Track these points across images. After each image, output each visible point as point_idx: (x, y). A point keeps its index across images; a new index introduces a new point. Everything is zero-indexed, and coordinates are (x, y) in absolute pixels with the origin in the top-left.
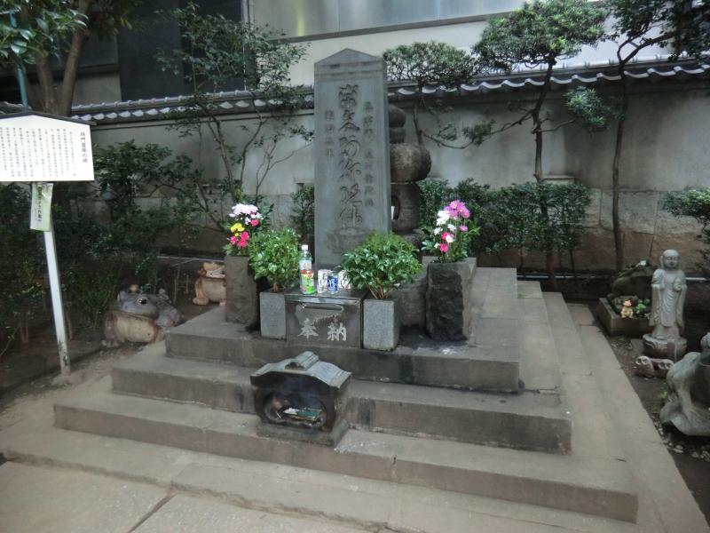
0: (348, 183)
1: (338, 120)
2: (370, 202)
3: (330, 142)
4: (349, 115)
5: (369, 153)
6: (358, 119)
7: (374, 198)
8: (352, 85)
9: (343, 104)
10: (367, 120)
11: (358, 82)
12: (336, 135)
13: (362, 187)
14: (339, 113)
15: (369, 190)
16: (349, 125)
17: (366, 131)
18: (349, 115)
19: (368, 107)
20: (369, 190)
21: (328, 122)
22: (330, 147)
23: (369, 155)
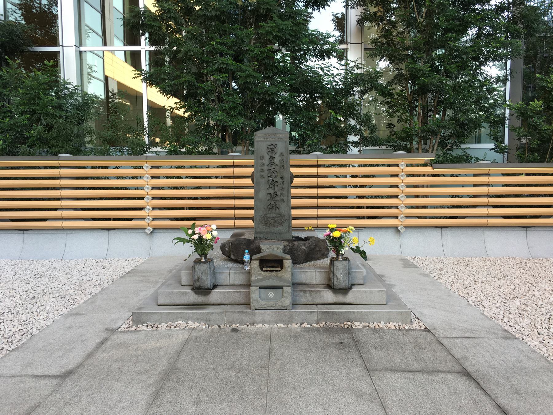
0: (271, 191)
1: (267, 161)
2: (283, 201)
3: (262, 171)
4: (272, 158)
5: (282, 177)
6: (277, 160)
7: (284, 198)
8: (274, 144)
9: (269, 153)
10: (282, 161)
11: (277, 143)
12: (266, 168)
13: (278, 193)
14: (267, 157)
15: (282, 194)
16: (272, 163)
17: (281, 166)
18: (272, 158)
19: (282, 155)
20: (282, 194)
21: (261, 161)
22: (262, 174)
23: (282, 178)
